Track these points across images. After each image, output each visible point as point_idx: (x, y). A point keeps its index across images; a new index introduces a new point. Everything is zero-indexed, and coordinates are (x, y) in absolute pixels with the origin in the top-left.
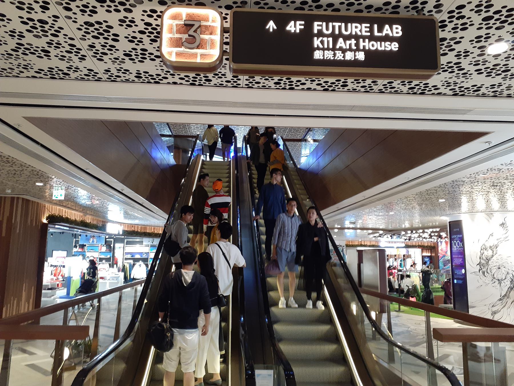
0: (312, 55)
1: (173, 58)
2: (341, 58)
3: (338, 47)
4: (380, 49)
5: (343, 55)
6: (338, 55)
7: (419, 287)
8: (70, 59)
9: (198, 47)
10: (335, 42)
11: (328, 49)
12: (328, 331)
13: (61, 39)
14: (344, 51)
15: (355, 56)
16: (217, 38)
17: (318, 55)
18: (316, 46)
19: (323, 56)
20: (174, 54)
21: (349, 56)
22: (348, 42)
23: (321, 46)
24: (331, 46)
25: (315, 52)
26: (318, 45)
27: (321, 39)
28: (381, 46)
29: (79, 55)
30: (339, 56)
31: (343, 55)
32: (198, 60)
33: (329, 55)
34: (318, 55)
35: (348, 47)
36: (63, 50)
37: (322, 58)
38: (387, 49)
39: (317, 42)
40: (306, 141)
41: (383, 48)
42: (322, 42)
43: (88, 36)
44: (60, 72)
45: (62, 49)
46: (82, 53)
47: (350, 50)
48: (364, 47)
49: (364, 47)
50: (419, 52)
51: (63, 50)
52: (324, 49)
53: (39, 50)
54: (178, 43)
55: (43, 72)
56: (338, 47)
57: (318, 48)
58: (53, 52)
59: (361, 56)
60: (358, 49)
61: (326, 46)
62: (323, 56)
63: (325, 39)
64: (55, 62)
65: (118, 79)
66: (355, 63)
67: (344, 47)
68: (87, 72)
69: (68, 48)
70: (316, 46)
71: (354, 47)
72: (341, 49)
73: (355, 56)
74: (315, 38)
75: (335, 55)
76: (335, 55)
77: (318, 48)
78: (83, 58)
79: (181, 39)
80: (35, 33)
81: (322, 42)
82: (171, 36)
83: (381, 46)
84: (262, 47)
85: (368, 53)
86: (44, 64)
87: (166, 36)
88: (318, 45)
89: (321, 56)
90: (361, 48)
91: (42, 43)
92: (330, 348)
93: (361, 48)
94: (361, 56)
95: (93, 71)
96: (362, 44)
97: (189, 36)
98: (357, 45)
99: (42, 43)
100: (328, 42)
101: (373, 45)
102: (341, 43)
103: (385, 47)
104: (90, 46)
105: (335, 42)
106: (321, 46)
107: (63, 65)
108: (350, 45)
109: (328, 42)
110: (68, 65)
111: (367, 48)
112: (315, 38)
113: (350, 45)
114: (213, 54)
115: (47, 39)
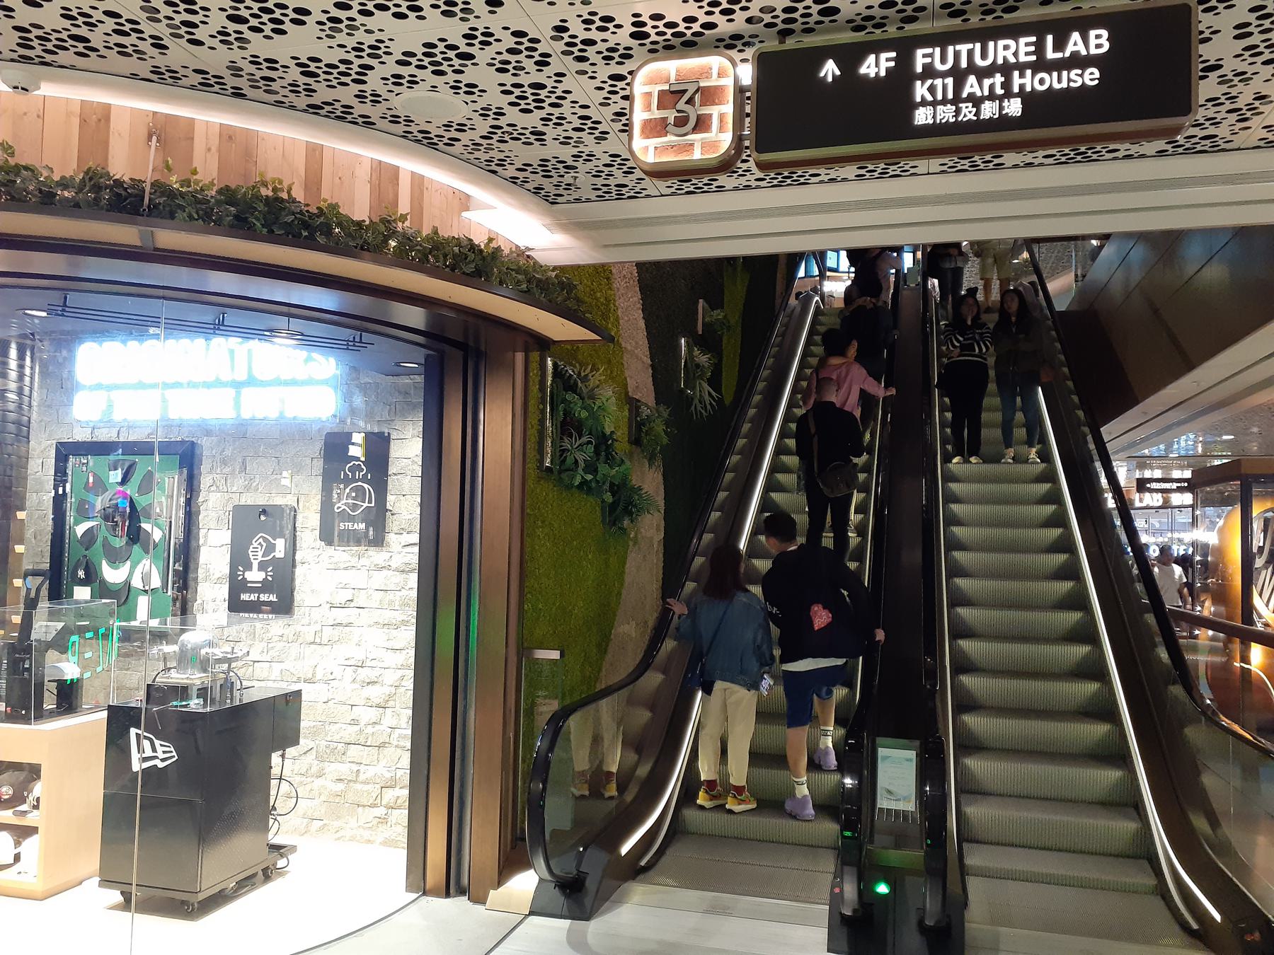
0: (910, 117)
1: (650, 158)
2: (971, 117)
3: (965, 95)
4: (1056, 86)
5: (974, 110)
6: (964, 111)
7: (104, 564)
8: (579, 141)
9: (696, 129)
10: (958, 86)
11: (944, 102)
12: (1095, 694)
13: (566, 109)
14: (976, 101)
15: (1001, 108)
16: (728, 108)
17: (922, 116)
18: (918, 99)
19: (934, 117)
20: (651, 150)
21: (989, 110)
22: (987, 82)
23: (929, 98)
24: (950, 96)
25: (917, 112)
26: (923, 97)
27: (929, 82)
28: (1059, 81)
29: (596, 132)
30: (968, 112)
31: (974, 110)
32: (697, 155)
33: (946, 114)
34: (922, 116)
35: (986, 93)
36: (569, 127)
37: (930, 121)
38: (1072, 84)
39: (921, 90)
40: (218, 379)
41: (1064, 85)
42: (932, 90)
43: (614, 98)
44: (560, 166)
45: (566, 126)
46: (601, 128)
47: (992, 96)
48: (1022, 87)
49: (1022, 87)
50: (1150, 83)
51: (569, 127)
52: (934, 104)
53: (527, 132)
54: (656, 128)
55: (530, 169)
56: (965, 95)
57: (924, 103)
58: (550, 132)
59: (1014, 107)
60: (1008, 94)
61: (940, 97)
62: (934, 117)
63: (938, 82)
64: (552, 150)
65: (560, 199)
66: (1003, 122)
67: (979, 94)
68: (608, 160)
69: (577, 123)
70: (918, 99)
71: (999, 91)
72: (972, 98)
73: (1001, 108)
74: (919, 83)
75: (958, 112)
76: (958, 112)
77: (924, 103)
78: (603, 137)
79: (665, 119)
80: (523, 106)
81: (932, 90)
82: (646, 116)
83: (1059, 81)
84: (808, 113)
85: (1029, 98)
86: (534, 154)
87: (639, 116)
88: (923, 97)
89: (930, 117)
90: (1016, 90)
91: (533, 120)
92: (1098, 730)
93: (1016, 90)
94: (1014, 107)
95: (619, 156)
96: (1017, 81)
97: (678, 111)
98: (1007, 85)
99: (533, 120)
100: (945, 87)
101: (1042, 82)
102: (971, 85)
103: (1069, 80)
104: (617, 114)
105: (958, 86)
106: (929, 98)
107: (566, 153)
108: (992, 87)
109: (945, 87)
110: (575, 151)
111: (1028, 89)
112: (919, 83)
113: (992, 87)
114: (720, 139)
115: (543, 114)
